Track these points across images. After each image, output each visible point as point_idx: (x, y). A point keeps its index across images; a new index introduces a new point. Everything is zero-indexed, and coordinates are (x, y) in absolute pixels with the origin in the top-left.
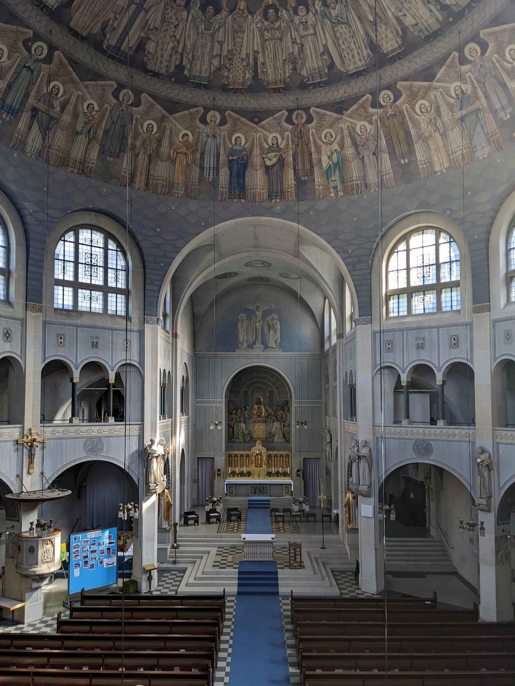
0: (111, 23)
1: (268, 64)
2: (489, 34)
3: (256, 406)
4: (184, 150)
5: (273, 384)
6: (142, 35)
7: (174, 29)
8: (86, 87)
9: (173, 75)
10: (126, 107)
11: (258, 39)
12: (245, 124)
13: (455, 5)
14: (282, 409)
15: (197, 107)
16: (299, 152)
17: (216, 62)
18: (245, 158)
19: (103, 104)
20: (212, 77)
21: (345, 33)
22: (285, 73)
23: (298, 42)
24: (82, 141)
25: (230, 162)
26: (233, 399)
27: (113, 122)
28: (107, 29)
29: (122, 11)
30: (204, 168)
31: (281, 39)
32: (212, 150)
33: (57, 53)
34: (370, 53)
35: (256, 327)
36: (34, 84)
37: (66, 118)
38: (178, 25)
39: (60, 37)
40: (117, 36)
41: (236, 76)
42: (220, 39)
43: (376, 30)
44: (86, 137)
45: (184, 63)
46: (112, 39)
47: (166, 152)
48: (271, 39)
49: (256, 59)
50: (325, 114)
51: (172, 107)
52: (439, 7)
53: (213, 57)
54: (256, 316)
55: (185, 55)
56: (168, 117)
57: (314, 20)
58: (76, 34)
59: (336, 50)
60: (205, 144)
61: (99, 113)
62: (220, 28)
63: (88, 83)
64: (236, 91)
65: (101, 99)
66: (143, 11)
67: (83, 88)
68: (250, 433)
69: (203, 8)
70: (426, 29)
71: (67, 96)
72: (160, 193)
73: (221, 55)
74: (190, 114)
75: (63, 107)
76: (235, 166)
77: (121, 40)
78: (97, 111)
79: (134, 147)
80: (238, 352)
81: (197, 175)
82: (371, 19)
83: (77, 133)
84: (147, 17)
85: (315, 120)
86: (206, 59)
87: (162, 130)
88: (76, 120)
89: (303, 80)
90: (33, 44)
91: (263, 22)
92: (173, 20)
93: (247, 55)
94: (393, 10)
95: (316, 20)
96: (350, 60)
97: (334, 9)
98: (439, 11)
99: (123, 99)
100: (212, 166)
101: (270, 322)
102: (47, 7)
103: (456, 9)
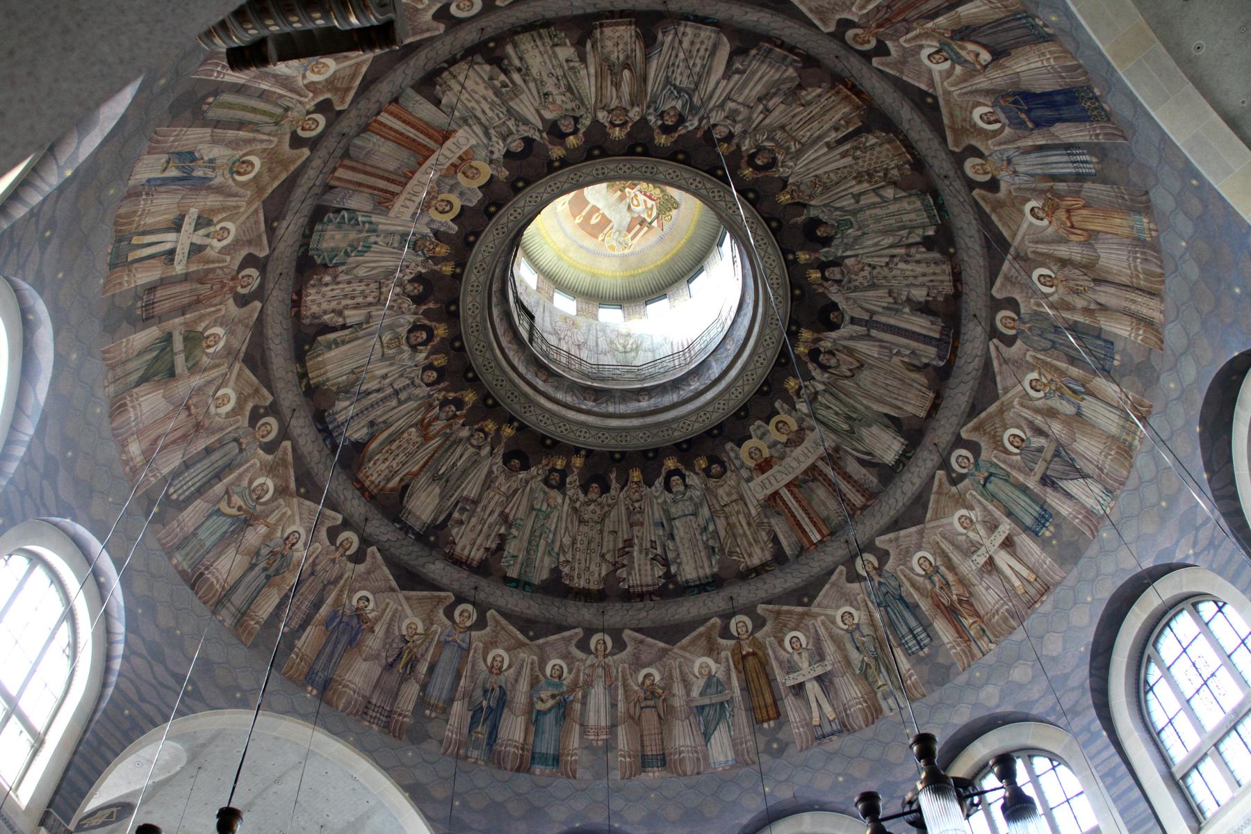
0: (906, 360)
1: (831, 123)
2: (428, 30)
4: (1062, 214)
6: (907, 310)
7: (878, 269)
8: (1006, 390)
9: (944, 252)
10: (1024, 323)
11: (810, 155)
12: (952, 115)
13: (477, 63)
15: (976, 203)
16: (912, 14)
17: (889, 193)
18: (1011, 99)
19: (1027, 362)
20: (914, 191)
21: (681, 74)
22: (819, 96)
23: (761, 107)
24: (1091, 408)
25: (1038, 125)
27: (1054, 345)
28: (916, 362)
29: (886, 348)
30: (1078, 174)
31: (783, 128)
32: (1040, 160)
33: (964, 435)
34: (660, 36)
36: (1008, 474)
37: (1056, 428)
38: (869, 265)
39: (942, 432)
40: (922, 346)
41: (887, 156)
42: (852, 201)
43: (627, 57)
44: (1083, 399)
45: (918, 239)
46: (929, 354)
47: (1077, 249)
48: (794, 139)
49: (840, 142)
50: (811, 10)
51: (996, 246)
52: (506, 62)
53: (885, 200)
55: (905, 241)
56: (1016, 250)
57: (714, 114)
58: (935, 408)
59: (715, 63)
60: (1032, 175)
61: (1043, 371)
62: (837, 209)
63: (999, 386)
64: (909, 146)
65: (1021, 366)
66: (875, 318)
67: (1009, 395)
69: (826, 242)
70: (541, 37)
71: (1023, 424)
72: (1161, 267)
73: (874, 190)
74: (994, 210)
75: (1039, 432)
76: (1039, 113)
77: (926, 339)
78: (1040, 374)
79: (1086, 311)
81: (1097, 186)
82: (626, 73)
83: (1079, 414)
84: (880, 310)
85: (838, 17)
86: (893, 208)
87: (1045, 259)
88: (1058, 413)
89: (803, 68)
90: (954, 471)
91: (783, 162)
92: (865, 273)
93: (843, 155)
94: (583, 73)
95: (711, 110)
96: (702, 43)
97: (674, 108)
98: (508, 57)
99: (1013, 328)
100: (1065, 159)
102: (905, 451)
103: (479, 58)
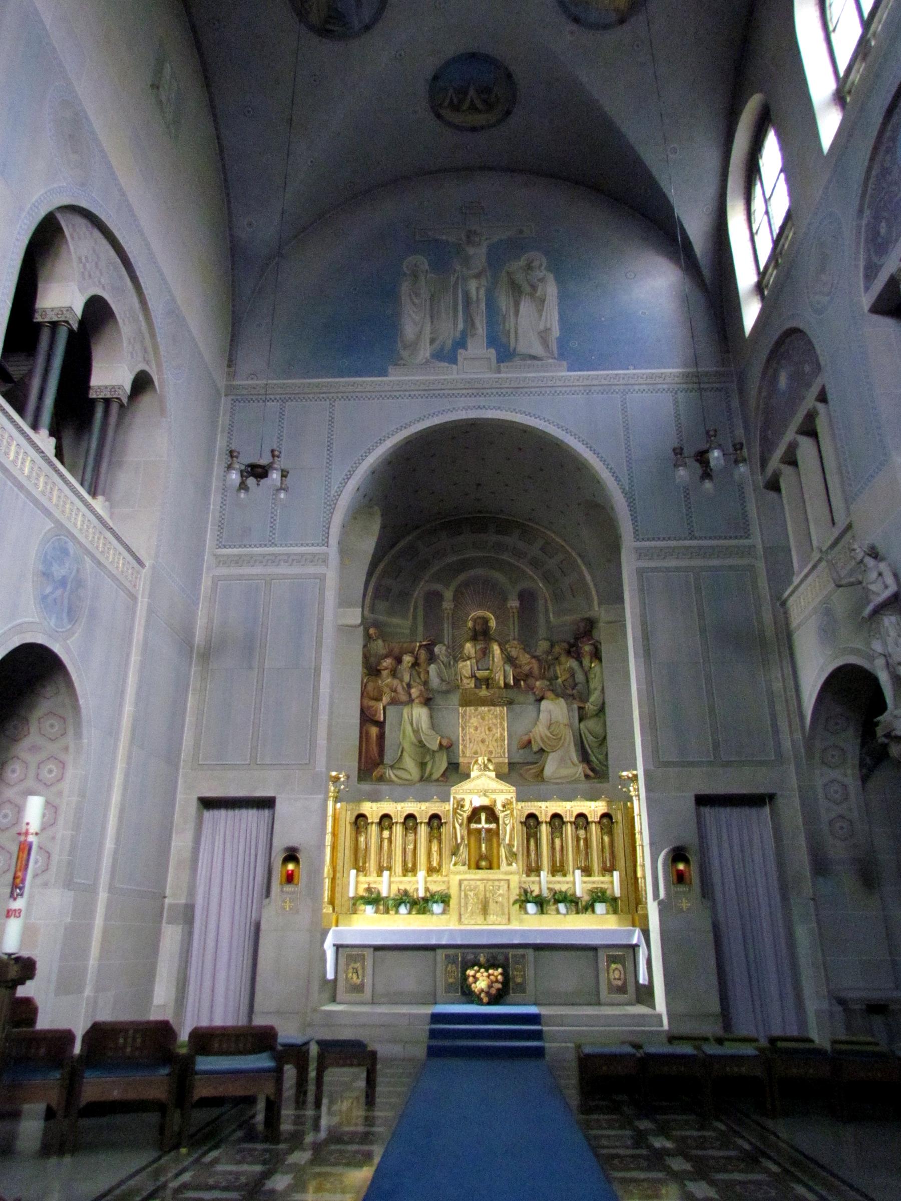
3: (469, 648)
5: (535, 563)
14: (573, 651)
26: (382, 618)
35: (467, 295)
54: (466, 261)
68: (448, 748)
80: (395, 376)
101: (520, 277)
